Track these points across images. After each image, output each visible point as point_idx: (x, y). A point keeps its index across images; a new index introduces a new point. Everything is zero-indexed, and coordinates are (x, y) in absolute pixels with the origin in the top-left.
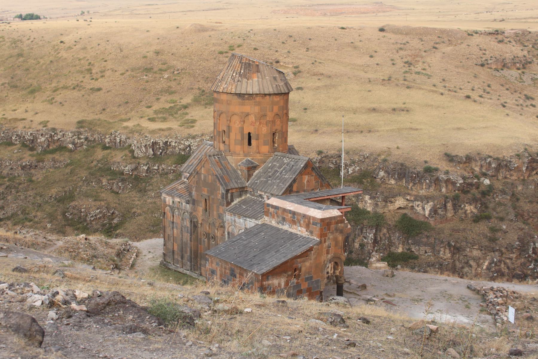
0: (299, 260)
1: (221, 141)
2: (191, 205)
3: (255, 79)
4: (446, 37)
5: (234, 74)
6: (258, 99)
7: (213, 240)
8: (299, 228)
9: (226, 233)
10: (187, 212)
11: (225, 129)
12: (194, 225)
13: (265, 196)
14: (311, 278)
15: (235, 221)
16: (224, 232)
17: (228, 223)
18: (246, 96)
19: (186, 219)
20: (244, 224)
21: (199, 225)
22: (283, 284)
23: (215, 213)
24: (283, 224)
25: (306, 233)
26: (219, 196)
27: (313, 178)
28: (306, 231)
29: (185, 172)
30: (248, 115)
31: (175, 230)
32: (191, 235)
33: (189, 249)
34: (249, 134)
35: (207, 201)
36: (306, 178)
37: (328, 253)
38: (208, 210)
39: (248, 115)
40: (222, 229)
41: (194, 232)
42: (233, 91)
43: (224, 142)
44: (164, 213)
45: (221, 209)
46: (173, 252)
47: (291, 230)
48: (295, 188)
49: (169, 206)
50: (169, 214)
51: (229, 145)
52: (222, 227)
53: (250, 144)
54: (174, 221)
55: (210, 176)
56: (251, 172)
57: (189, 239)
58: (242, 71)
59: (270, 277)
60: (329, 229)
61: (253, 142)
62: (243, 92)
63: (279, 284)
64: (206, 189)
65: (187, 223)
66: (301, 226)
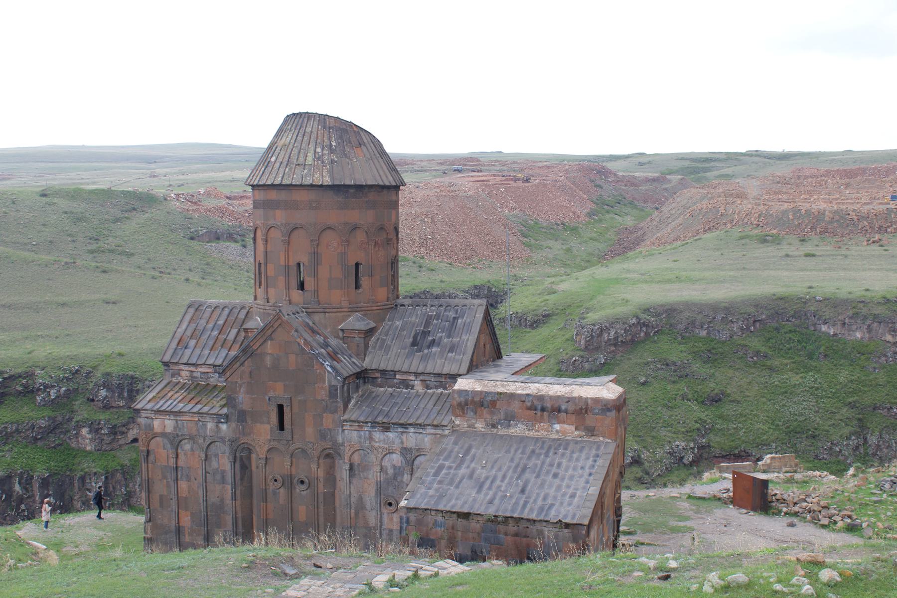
1: (294, 283)
2: (233, 425)
4: (140, 201)
5: (319, 150)
6: (372, 196)
7: (303, 487)
8: (557, 427)
10: (222, 440)
11: (304, 259)
13: (417, 383)
15: (371, 438)
17: (351, 446)
18: (352, 191)
19: (217, 455)
20: (397, 441)
23: (310, 430)
24: (509, 426)
25: (577, 433)
26: (323, 394)
28: (576, 429)
29: (177, 363)
30: (355, 228)
31: (183, 485)
32: (234, 486)
35: (286, 410)
39: (355, 228)
40: (328, 460)
41: (242, 479)
42: (327, 181)
43: (301, 286)
44: (148, 452)
45: (328, 421)
47: (532, 434)
49: (164, 435)
50: (162, 451)
51: (317, 291)
52: (328, 456)
53: (357, 287)
54: (181, 463)
55: (292, 358)
56: (367, 339)
58: (334, 144)
61: (364, 281)
62: (348, 182)
64: (280, 385)
65: (224, 462)
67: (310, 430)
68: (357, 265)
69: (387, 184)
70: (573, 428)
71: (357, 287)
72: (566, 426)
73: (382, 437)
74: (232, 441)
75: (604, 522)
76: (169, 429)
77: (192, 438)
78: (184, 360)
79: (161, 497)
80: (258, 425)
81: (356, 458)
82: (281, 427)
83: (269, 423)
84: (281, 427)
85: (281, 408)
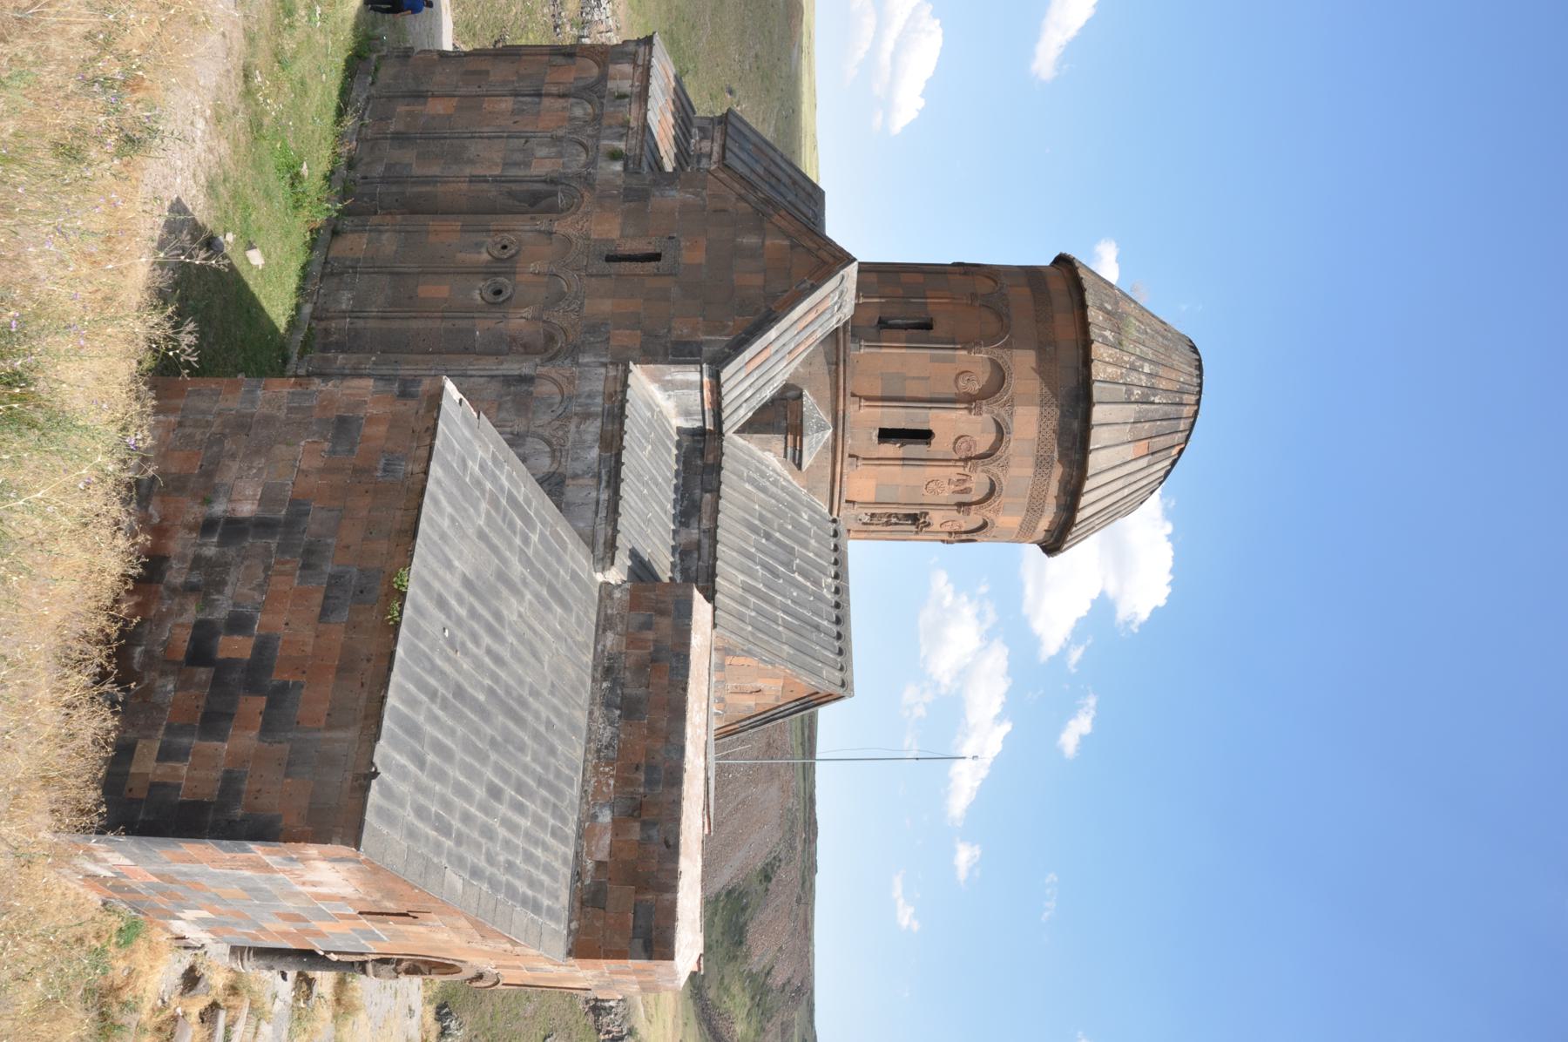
3: (1129, 452)
9: (526, 369)
12: (538, 199)
15: (587, 416)
16: (528, 350)
19: (560, 155)
20: (579, 467)
21: (542, 223)
25: (590, 865)
28: (600, 865)
31: (507, 104)
32: (497, 180)
33: (435, 170)
38: (616, 265)
46: (419, 96)
49: (604, 77)
53: (886, 435)
54: (546, 102)
57: (480, 171)
59: (351, 865)
61: (891, 449)
62: (1098, 413)
65: (544, 164)
66: (618, 826)
67: (606, 306)
68: (925, 436)
70: (603, 855)
71: (886, 435)
72: (607, 839)
73: (589, 438)
74: (587, 180)
75: (365, 922)
76: (611, 85)
77: (597, 119)
78: (729, 143)
79: (487, 72)
80: (619, 220)
81: (545, 388)
82: (611, 259)
83: (622, 236)
84: (611, 259)
85: (656, 257)
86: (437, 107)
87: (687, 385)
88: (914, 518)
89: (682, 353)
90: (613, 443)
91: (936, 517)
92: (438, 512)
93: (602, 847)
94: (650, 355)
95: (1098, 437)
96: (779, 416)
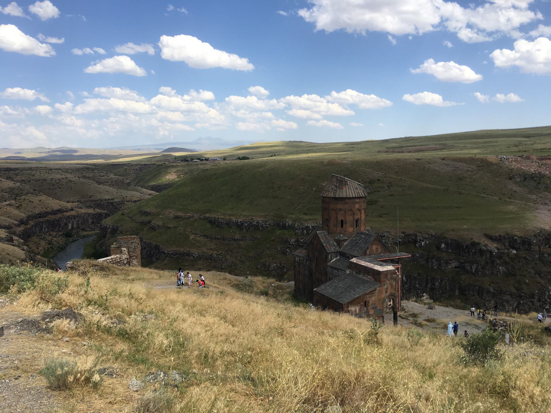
0: (368, 296)
14: (376, 307)
22: (358, 310)
27: (379, 247)
31: (301, 277)
34: (342, 221)
36: (374, 247)
37: (386, 292)
48: (368, 252)
53: (342, 226)
60: (387, 278)
61: (344, 226)
62: (337, 196)
63: (356, 311)
68: (342, 221)
69: (351, 196)
86: (301, 287)
87: (331, 257)
88: (357, 221)
89: (327, 257)
90: (335, 269)
91: (356, 217)
92: (324, 292)
93: (372, 278)
94: (326, 262)
95: (341, 196)
96: (339, 243)
